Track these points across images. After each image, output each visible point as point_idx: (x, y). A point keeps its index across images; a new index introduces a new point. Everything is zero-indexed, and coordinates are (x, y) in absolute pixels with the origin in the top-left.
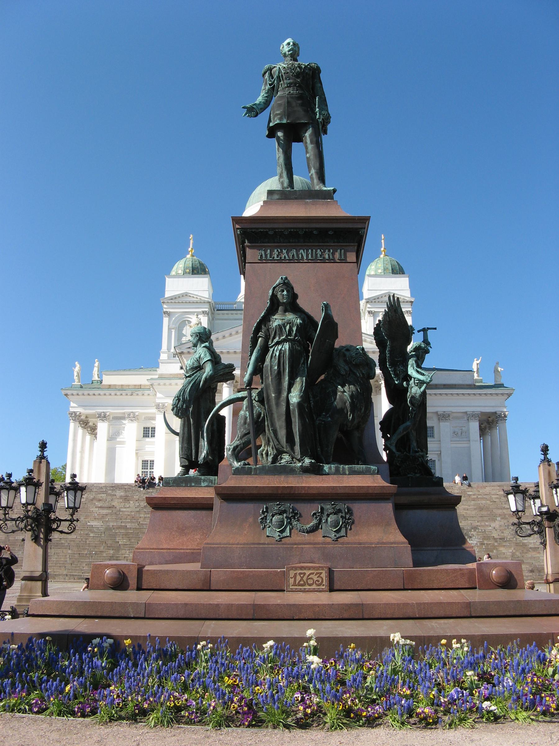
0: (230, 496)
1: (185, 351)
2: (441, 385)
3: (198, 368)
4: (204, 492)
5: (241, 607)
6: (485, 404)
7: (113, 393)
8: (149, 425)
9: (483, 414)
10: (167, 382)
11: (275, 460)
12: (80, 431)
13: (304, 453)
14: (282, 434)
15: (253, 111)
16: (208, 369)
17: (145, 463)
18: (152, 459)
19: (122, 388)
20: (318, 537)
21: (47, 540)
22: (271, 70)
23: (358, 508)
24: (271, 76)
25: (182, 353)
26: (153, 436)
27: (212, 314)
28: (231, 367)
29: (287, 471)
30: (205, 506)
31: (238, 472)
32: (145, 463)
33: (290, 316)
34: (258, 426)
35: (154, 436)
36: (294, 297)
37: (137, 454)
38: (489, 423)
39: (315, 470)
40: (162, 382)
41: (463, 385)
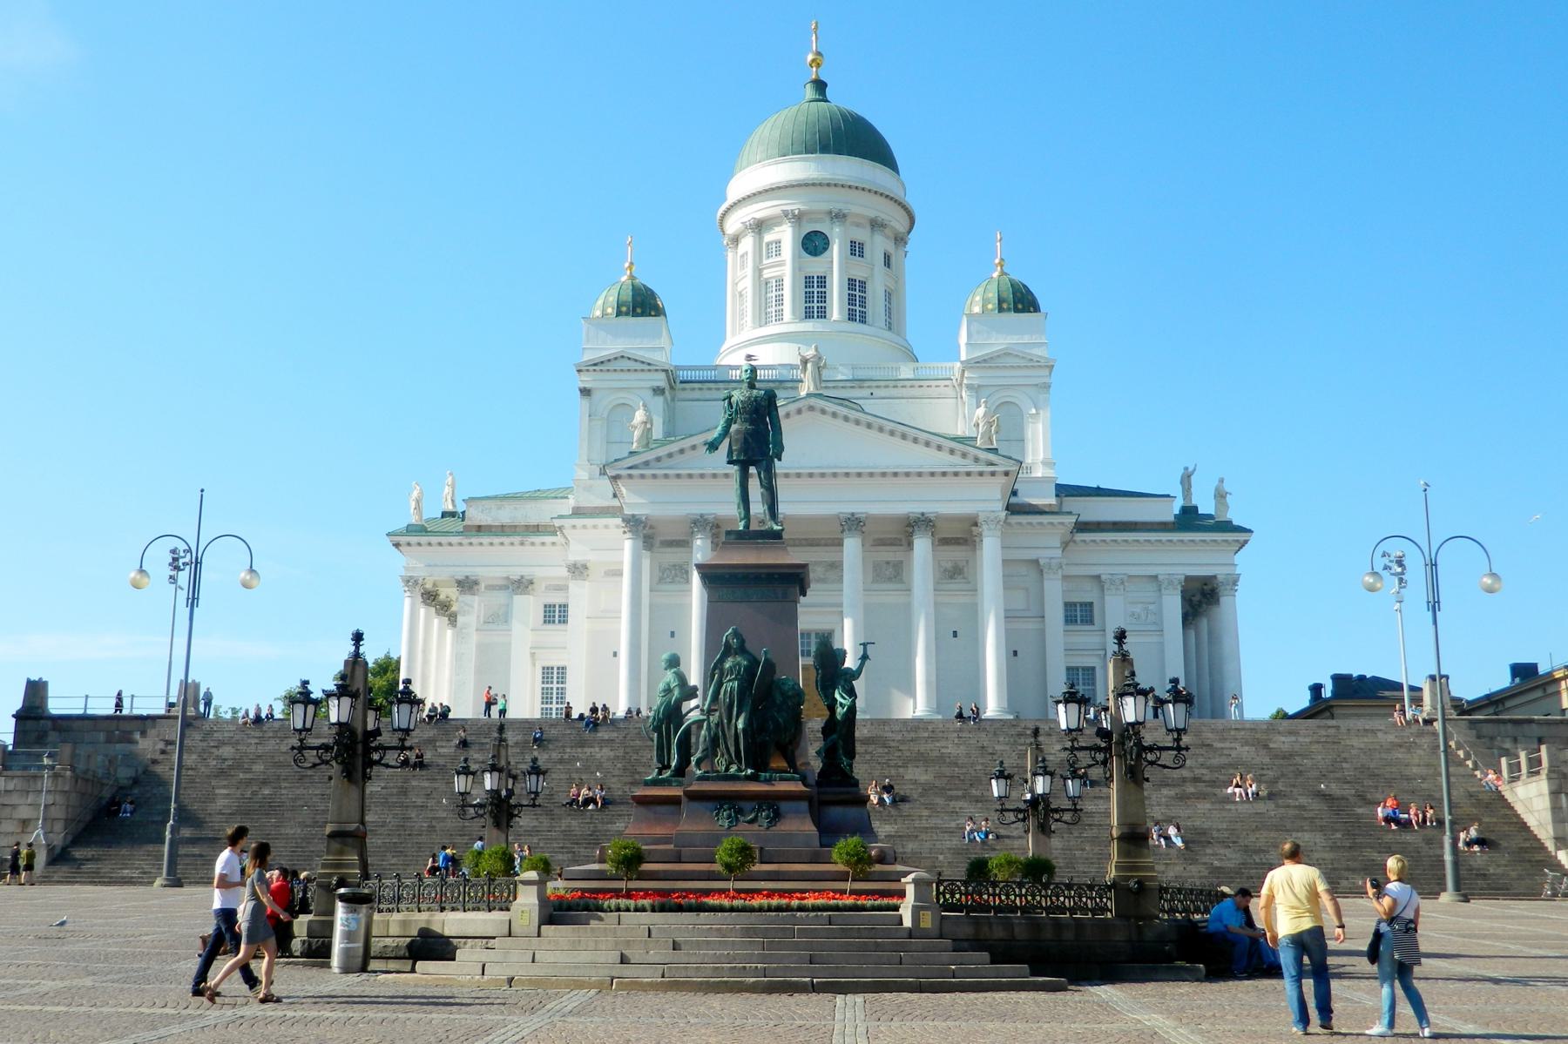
0: (694, 797)
1: (624, 473)
2: (1107, 523)
3: (668, 690)
4: (675, 791)
5: (700, 872)
6: (1194, 557)
7: (486, 540)
8: (556, 599)
9: (1188, 579)
10: (589, 522)
11: (727, 769)
12: (422, 611)
13: (747, 766)
14: (732, 750)
15: (713, 446)
16: (676, 693)
17: (547, 672)
18: (561, 664)
19: (503, 530)
20: (755, 826)
21: (509, 826)
22: (730, 398)
23: (784, 806)
24: (730, 404)
25: (615, 478)
26: (564, 620)
27: (672, 388)
28: (695, 688)
29: (734, 778)
30: (674, 801)
31: (701, 778)
32: (547, 672)
33: (739, 659)
34: (714, 742)
35: (565, 622)
36: (742, 642)
37: (533, 655)
38: (1201, 598)
39: (753, 778)
40: (579, 522)
41: (1152, 524)
